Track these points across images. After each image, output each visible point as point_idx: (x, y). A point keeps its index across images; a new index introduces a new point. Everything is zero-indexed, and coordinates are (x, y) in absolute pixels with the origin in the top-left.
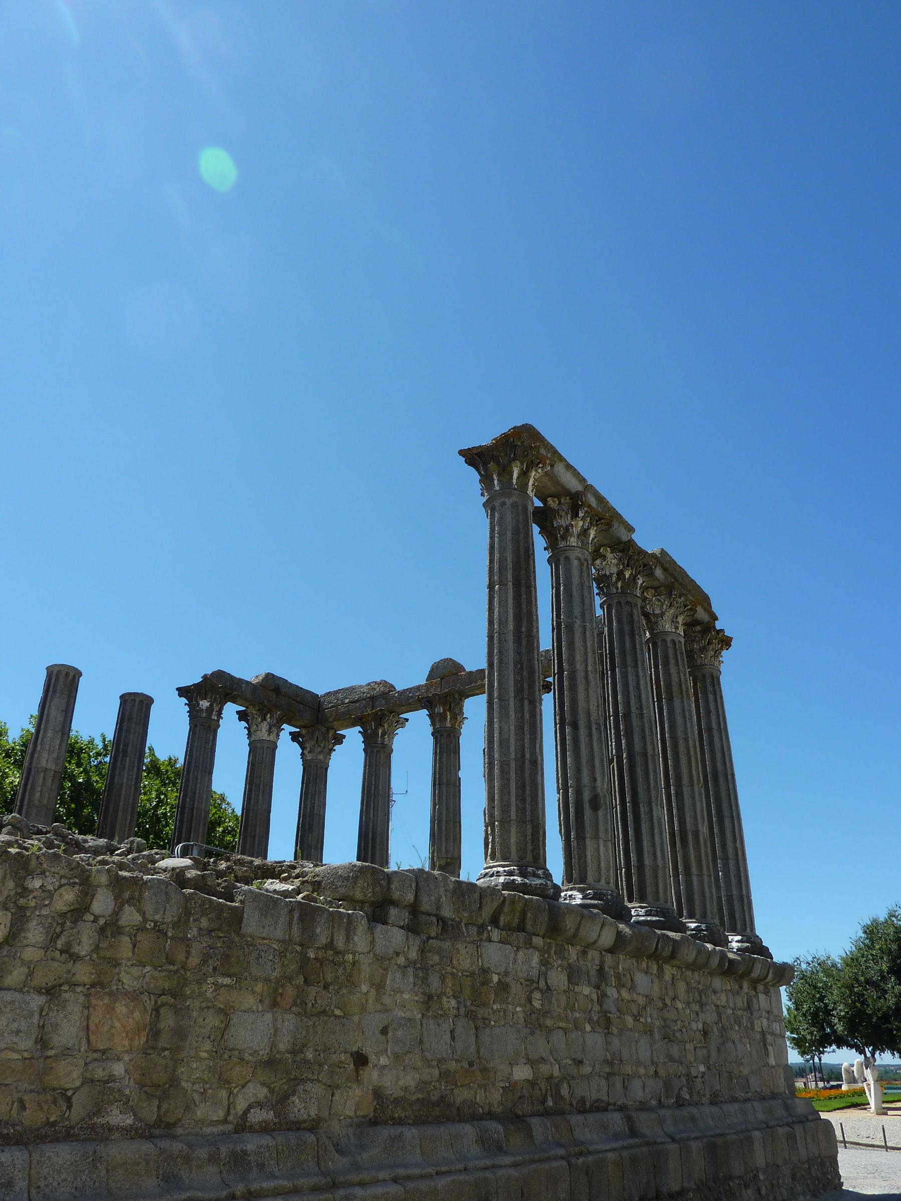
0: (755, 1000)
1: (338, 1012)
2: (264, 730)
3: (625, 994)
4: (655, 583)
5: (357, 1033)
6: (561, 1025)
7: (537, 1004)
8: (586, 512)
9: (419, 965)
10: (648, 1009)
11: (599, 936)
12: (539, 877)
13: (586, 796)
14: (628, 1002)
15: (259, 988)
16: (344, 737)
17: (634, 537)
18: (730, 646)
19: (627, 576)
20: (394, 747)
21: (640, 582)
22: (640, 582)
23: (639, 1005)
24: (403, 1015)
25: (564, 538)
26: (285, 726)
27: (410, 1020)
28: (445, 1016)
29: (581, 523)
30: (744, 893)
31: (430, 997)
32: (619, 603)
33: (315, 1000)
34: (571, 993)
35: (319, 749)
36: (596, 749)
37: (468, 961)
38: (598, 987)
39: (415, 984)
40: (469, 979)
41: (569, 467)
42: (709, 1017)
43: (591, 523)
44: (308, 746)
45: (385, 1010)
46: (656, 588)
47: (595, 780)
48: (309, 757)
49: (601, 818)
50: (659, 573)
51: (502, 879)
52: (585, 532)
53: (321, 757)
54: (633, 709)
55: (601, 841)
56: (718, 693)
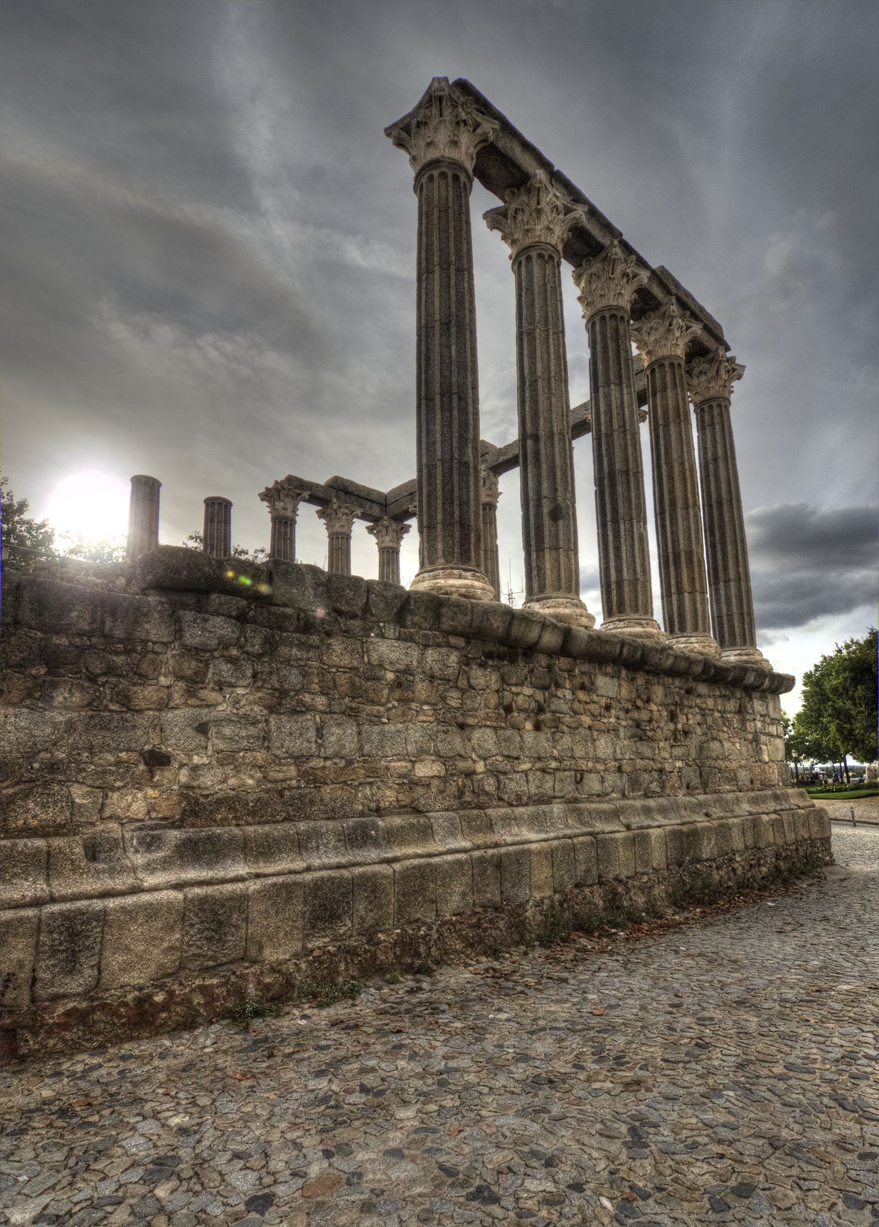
11: (540, 637)
16: (410, 526)
47: (556, 490)
49: (561, 527)
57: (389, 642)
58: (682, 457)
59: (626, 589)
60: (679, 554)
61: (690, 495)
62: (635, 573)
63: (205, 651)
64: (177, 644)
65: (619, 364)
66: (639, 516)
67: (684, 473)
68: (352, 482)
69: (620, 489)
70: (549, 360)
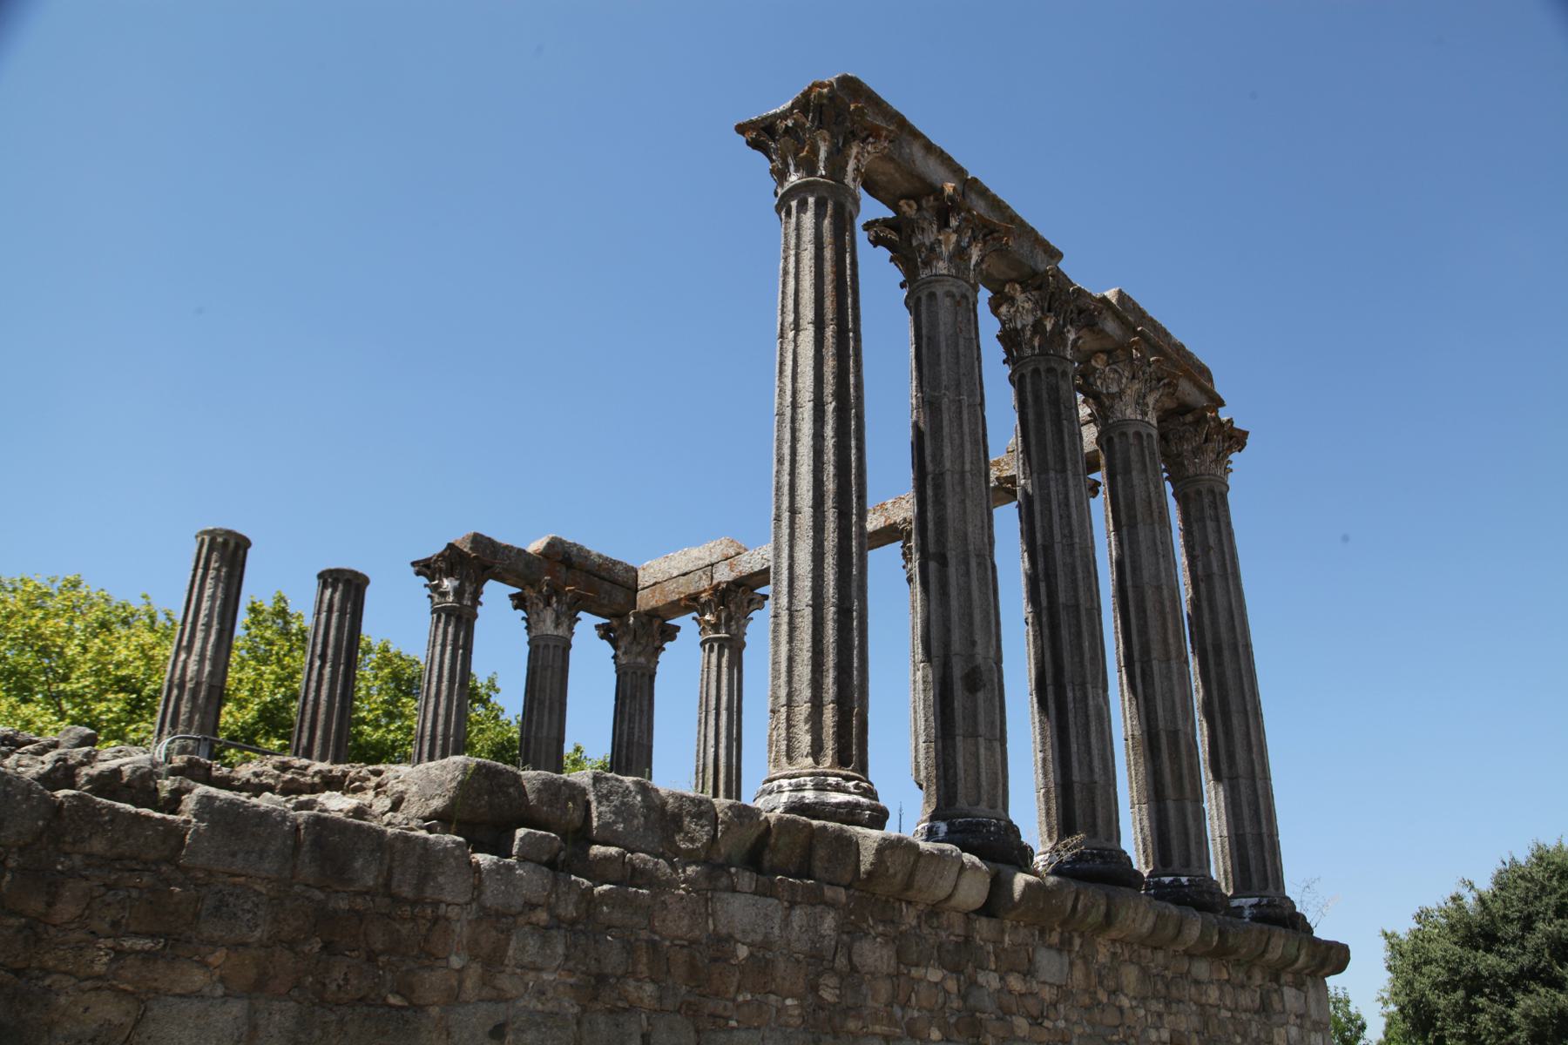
0: (1275, 997)
1: (394, 1000)
2: (548, 622)
3: (1015, 983)
4: (1109, 345)
5: (434, 1035)
6: (878, 1028)
7: (828, 995)
8: (965, 219)
9: (580, 927)
10: (1061, 1007)
11: (955, 887)
12: (846, 791)
13: (957, 672)
14: (1021, 995)
15: (217, 958)
16: (678, 628)
17: (1061, 265)
18: (1244, 445)
19: (1049, 328)
20: (746, 639)
21: (1072, 336)
22: (1072, 336)
23: (1043, 1000)
24: (540, 1007)
25: (927, 263)
26: (581, 614)
27: (552, 1014)
28: (631, 1009)
29: (954, 238)
30: (1264, 830)
31: (601, 978)
32: (1036, 371)
33: (346, 980)
34: (902, 979)
35: (640, 648)
36: (976, 594)
37: (686, 922)
38: (956, 970)
39: (567, 958)
40: (685, 951)
41: (929, 147)
42: (1186, 1021)
43: (974, 238)
44: (622, 644)
45: (500, 998)
46: (1109, 353)
47: (974, 643)
48: (623, 660)
50: (1111, 326)
51: (784, 798)
52: (960, 254)
53: (642, 660)
54: (1058, 537)
55: (981, 740)
56: (1222, 519)
57: (742, 897)
58: (1157, 576)
59: (1078, 796)
60: (1157, 734)
61: (1171, 640)
62: (1091, 770)
63: (505, 915)
64: (474, 906)
65: (1061, 440)
66: (1095, 678)
67: (1162, 604)
68: (581, 549)
69: (1064, 633)
70: (962, 445)
